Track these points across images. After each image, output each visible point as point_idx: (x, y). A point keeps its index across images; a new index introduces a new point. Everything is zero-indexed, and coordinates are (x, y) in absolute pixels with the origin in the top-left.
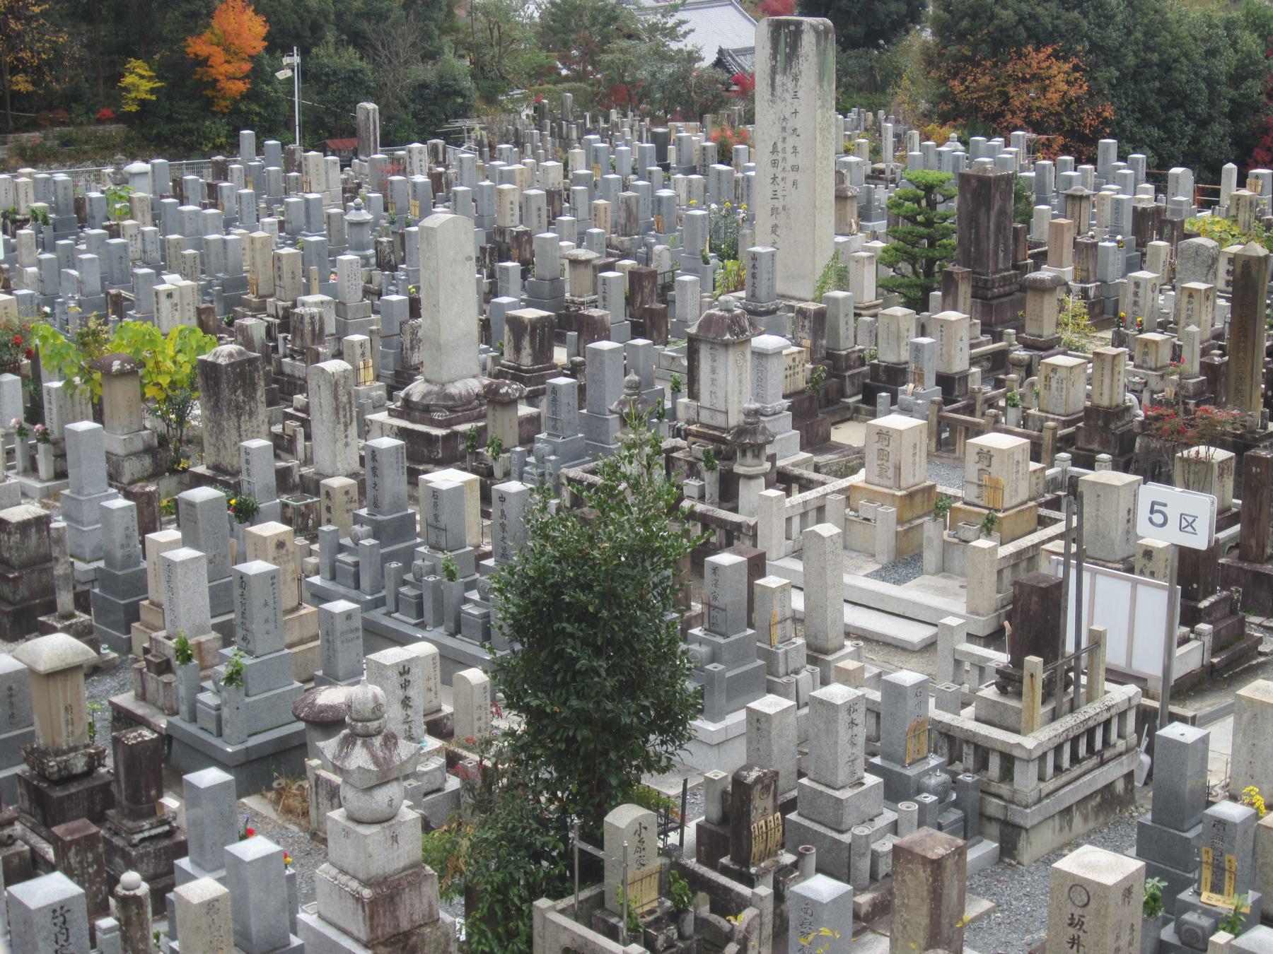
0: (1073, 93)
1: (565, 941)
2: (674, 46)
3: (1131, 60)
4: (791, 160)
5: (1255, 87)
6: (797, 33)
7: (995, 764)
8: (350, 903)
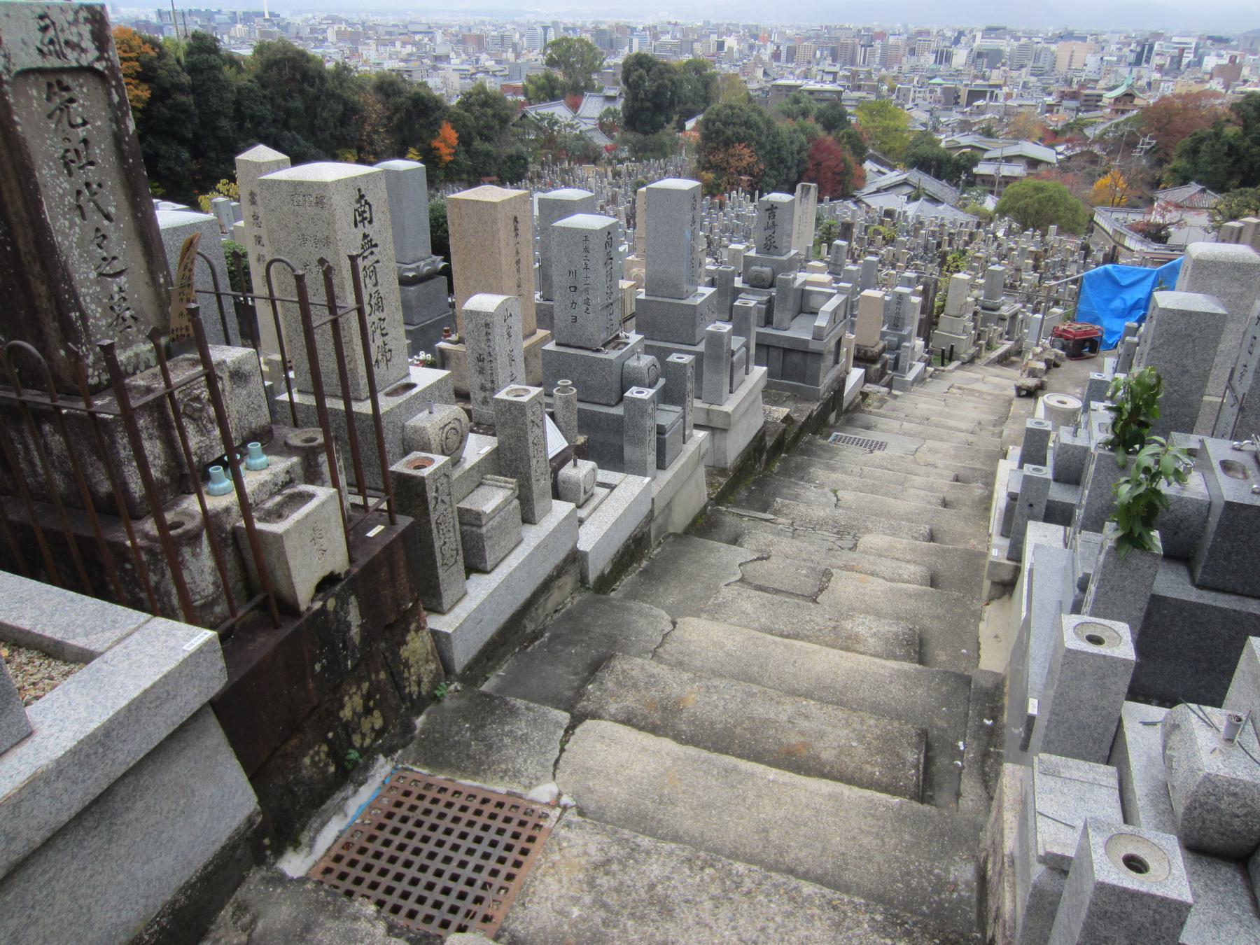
3: (768, 148)
5: (804, 154)
6: (809, 188)
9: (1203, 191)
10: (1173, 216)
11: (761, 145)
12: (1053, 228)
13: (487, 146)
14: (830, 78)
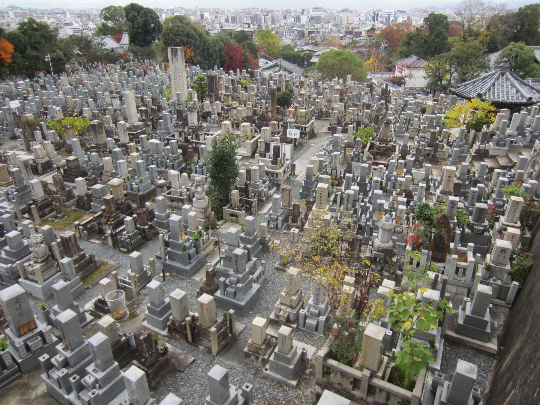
0: (192, 55)
1: (230, 213)
2: (104, 48)
3: (201, 48)
4: (178, 75)
5: (223, 52)
6: (177, 50)
7: (275, 176)
8: (200, 213)
9: (419, 59)
10: (406, 72)
11: (198, 48)
12: (349, 77)
13: (35, 53)
14: (247, 26)
